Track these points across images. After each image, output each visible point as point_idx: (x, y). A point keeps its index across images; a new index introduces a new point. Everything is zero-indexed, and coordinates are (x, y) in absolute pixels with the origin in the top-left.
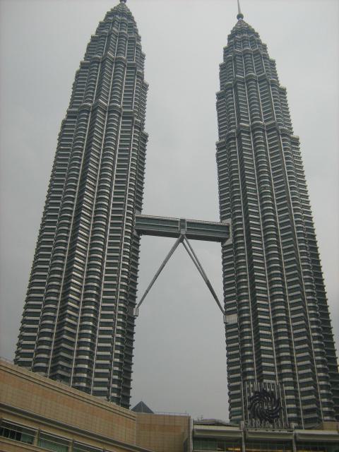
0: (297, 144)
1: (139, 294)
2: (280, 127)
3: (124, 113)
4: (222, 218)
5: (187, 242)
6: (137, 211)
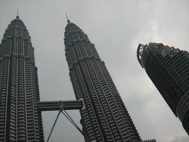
4: (77, 99)
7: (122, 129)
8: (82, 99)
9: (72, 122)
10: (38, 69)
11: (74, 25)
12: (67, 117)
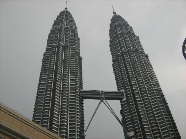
1: (86, 126)
4: (119, 90)
5: (106, 101)
6: (81, 89)
7: (161, 124)
8: (123, 90)
9: (112, 112)
10: (82, 59)
11: (119, 17)
12: (107, 106)
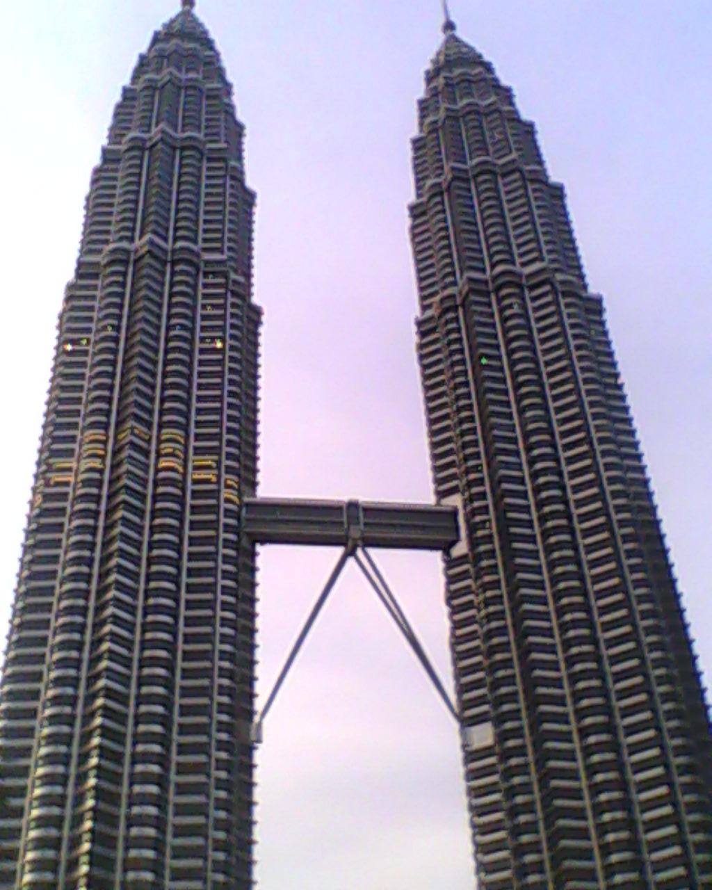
0: (600, 312)
2: (559, 277)
3: (207, 263)
4: (441, 495)
11: (477, 60)
